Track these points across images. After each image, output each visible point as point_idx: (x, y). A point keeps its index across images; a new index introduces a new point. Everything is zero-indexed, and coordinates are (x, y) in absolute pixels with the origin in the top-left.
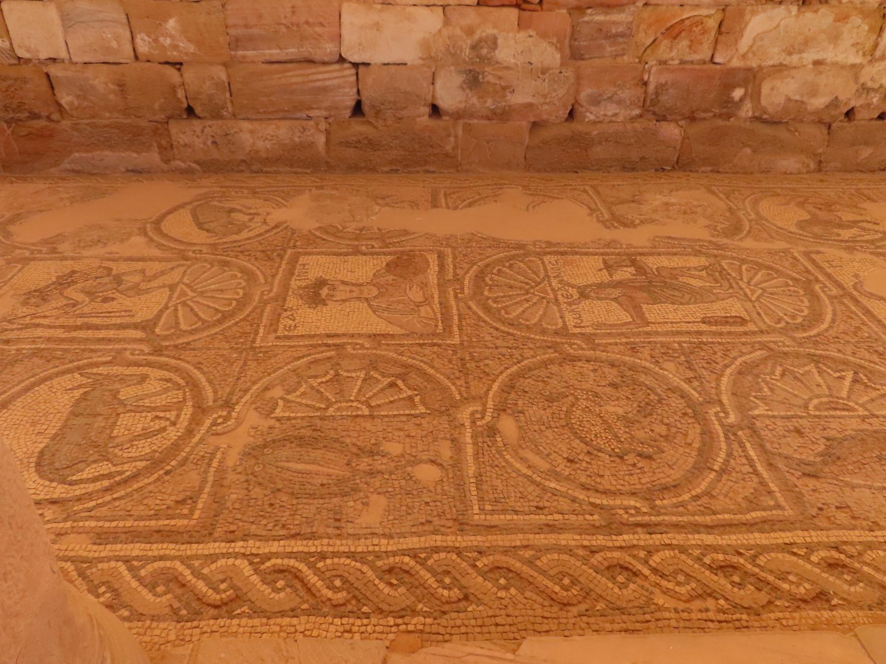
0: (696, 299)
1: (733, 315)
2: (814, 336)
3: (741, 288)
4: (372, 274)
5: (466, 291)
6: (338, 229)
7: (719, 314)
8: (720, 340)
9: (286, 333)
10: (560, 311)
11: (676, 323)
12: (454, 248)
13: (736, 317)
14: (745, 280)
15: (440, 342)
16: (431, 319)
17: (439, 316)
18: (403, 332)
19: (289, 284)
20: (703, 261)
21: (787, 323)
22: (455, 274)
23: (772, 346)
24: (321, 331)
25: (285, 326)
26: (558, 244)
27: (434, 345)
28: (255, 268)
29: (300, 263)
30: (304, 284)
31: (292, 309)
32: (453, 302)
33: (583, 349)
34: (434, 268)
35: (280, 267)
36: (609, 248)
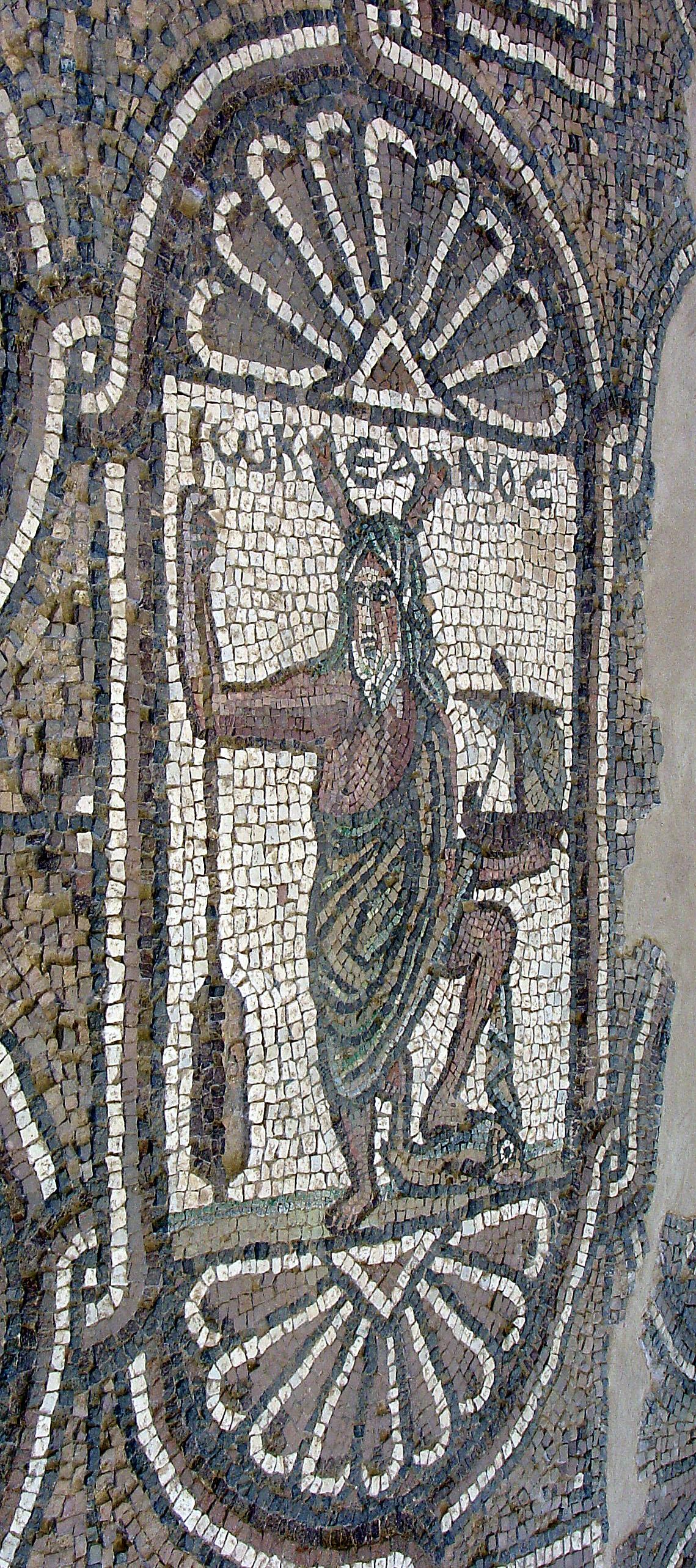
0: (339, 1007)
1: (257, 1138)
2: (132, 1446)
3: (396, 1231)
5: (394, 52)
7: (255, 1072)
8: (115, 1014)
10: (284, 394)
11: (210, 861)
13: (247, 1146)
14: (439, 1264)
20: (544, 1123)
21: (208, 1356)
23: (81, 1242)
26: (636, 557)
33: (74, 387)
36: (614, 760)
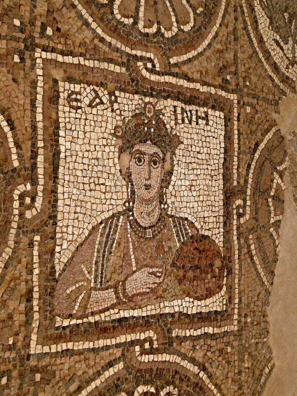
4: (182, 215)
5: (146, 358)
6: (280, 164)
12: (238, 334)
15: (35, 325)
16: (85, 308)
17: (91, 319)
19: (166, 98)
22: (182, 340)
24: (64, 144)
27: (29, 312)
28: (200, 49)
29: (210, 112)
30: (165, 119)
31: (112, 103)
32: (122, 339)
35: (204, 84)
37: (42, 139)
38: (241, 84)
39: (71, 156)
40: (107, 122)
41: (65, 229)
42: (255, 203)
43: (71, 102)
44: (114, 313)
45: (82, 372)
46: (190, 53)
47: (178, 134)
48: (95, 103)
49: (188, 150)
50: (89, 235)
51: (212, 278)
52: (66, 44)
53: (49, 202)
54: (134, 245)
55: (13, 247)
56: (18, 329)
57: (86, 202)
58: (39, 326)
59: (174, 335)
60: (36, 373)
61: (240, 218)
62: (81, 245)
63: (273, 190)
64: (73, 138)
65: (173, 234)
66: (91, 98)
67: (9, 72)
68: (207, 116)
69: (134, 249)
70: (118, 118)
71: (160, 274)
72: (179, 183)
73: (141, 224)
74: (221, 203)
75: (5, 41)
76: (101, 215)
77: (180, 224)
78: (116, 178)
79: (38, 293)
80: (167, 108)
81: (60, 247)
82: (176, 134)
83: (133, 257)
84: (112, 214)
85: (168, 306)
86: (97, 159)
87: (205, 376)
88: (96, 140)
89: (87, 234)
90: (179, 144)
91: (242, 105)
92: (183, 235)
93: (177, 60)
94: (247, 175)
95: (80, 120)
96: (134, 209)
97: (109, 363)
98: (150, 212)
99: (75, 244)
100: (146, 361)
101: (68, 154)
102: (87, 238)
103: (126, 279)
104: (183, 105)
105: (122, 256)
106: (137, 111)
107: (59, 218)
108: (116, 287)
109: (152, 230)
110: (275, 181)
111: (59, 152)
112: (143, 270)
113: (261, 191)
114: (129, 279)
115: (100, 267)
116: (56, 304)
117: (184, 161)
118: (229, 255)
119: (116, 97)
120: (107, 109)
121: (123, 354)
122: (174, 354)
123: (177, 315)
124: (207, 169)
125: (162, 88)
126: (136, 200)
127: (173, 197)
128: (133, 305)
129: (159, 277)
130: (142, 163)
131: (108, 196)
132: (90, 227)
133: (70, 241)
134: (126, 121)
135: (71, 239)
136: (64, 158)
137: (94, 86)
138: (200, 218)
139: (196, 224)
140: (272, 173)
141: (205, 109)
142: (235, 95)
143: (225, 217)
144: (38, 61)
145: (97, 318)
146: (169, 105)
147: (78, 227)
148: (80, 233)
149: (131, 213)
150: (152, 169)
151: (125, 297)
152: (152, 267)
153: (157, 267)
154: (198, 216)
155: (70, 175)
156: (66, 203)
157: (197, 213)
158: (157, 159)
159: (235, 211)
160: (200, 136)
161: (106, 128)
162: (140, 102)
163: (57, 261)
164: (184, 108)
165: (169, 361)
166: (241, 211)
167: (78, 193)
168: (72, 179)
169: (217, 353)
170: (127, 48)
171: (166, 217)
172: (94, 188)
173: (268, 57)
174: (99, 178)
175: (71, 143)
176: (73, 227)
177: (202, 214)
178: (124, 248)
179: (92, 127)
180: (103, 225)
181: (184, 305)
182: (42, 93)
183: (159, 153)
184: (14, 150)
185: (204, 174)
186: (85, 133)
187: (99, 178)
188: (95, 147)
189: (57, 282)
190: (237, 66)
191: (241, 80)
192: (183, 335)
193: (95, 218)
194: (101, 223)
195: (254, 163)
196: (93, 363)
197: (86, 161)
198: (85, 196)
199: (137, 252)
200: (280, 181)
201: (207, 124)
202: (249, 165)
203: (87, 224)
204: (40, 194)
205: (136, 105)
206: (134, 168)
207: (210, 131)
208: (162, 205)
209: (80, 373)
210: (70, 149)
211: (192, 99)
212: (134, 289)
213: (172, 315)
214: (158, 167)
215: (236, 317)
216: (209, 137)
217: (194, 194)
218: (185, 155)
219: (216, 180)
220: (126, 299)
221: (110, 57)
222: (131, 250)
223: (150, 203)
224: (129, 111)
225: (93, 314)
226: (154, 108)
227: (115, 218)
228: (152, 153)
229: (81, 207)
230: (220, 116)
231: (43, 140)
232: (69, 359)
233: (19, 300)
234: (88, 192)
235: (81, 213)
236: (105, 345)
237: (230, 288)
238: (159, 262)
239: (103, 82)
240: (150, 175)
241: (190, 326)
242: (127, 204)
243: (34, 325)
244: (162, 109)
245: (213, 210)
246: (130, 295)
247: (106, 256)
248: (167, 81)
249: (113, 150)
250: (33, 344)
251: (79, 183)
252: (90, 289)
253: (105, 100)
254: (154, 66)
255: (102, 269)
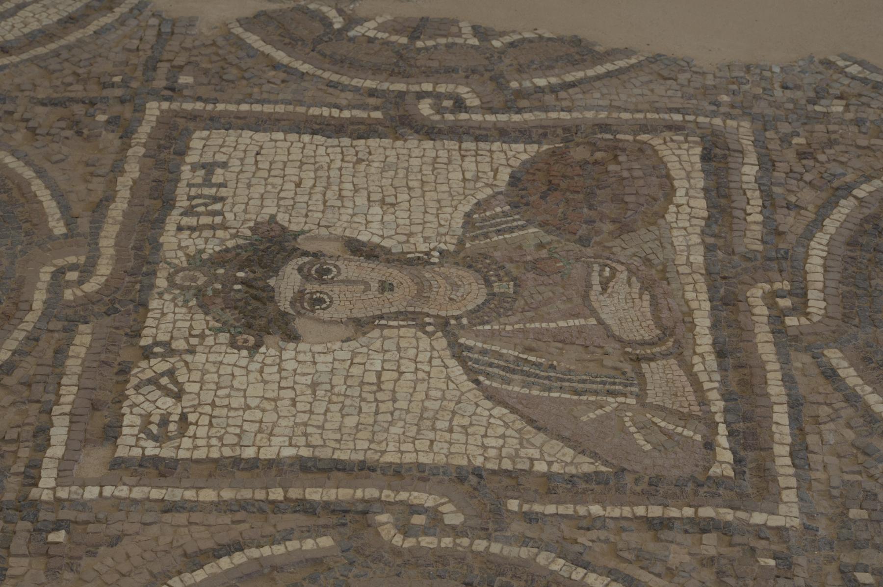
4: (458, 222)
5: (816, 304)
6: (326, 22)
9: (151, 449)
12: (764, 124)
15: (728, 515)
16: (691, 416)
17: (718, 406)
18: (587, 466)
19: (157, 247)
22: (774, 231)
24: (279, 448)
25: (146, 419)
28: (28, 173)
30: (212, 248)
31: (172, 352)
32: (767, 350)
34: (689, 204)
35: (117, 169)
37: (264, 492)
38: (118, 92)
39: (305, 435)
40: (221, 363)
41: (492, 453)
42: (428, 74)
43: (169, 434)
44: (703, 363)
45: (849, 431)
46: (38, 193)
47: (252, 224)
48: (171, 386)
49: (293, 206)
50: (506, 405)
51: (619, 163)
52: (17, 441)
53: (425, 480)
54: (532, 320)
55: (535, 550)
56: (738, 548)
57: (424, 409)
58: (732, 508)
59: (759, 247)
60: (847, 517)
61: (466, 107)
62: (531, 422)
63: (394, 38)
64: (260, 431)
65: (505, 239)
66: (158, 393)
67: (92, 554)
68: (203, 166)
69: (542, 319)
70: (210, 341)
71: (607, 269)
72: (375, 227)
73: (480, 301)
74: (428, 144)
75: (11, 559)
76: (458, 382)
77: (481, 228)
78: (365, 350)
79: (650, 507)
80: (183, 244)
81: (535, 462)
82: (250, 228)
83: (562, 324)
84: (454, 361)
85: (688, 258)
86: (314, 386)
87: (864, 186)
88: (267, 387)
89: (505, 411)
90: (276, 223)
91: (173, 91)
92: (506, 222)
93: (58, 220)
94: (356, 90)
95: (215, 417)
96: (443, 313)
97: (827, 377)
98: (451, 284)
99: (529, 432)
100: (823, 304)
101: (302, 441)
102: (513, 410)
103: (620, 340)
104: (175, 212)
105: (560, 345)
106: (190, 304)
107: (464, 462)
108: (639, 359)
109: (495, 282)
110: (371, 34)
111: (300, 458)
112: (596, 305)
113: (401, 64)
114: (617, 333)
115: (588, 386)
116: (676, 472)
117: (320, 215)
118: (559, 131)
119: (156, 344)
120: (187, 363)
121: (807, 349)
122: (807, 247)
123: (710, 240)
124: (340, 169)
125: (133, 252)
126: (418, 310)
127: (412, 240)
128: (680, 330)
129: (614, 271)
130: (325, 297)
131: (408, 366)
132: (488, 404)
133: (521, 444)
134: (217, 325)
135: (516, 441)
136: (311, 449)
137: (128, 386)
138: (464, 188)
139: (481, 196)
140: (352, 40)
141: (186, 168)
142: (148, 105)
143: (465, 137)
144: (63, 494)
145: (714, 395)
146: (174, 240)
147: (487, 428)
148: (502, 423)
149: (453, 322)
150: (340, 278)
151: (660, 341)
152: (589, 286)
153: (589, 275)
154: (461, 191)
155: (355, 439)
156: (427, 449)
157: (454, 194)
158: (314, 268)
159: (450, 117)
160: (254, 181)
161: (235, 365)
162: (167, 296)
163: (572, 470)
164: (182, 210)
165: (825, 258)
166: (448, 103)
167: (401, 424)
168: (364, 435)
169: (809, 163)
170: (27, 318)
171: (462, 255)
172: (390, 394)
173: (46, 35)
174: (362, 384)
175: (274, 435)
176: (485, 436)
177: (457, 185)
178: (540, 340)
179: (233, 393)
180: (481, 378)
181: (687, 224)
182: (146, 489)
183: (300, 263)
184: (293, 545)
185: (354, 176)
186: (248, 407)
187: (362, 384)
188: (284, 388)
189: (623, 470)
190: (72, 100)
191: (106, 93)
192: (758, 228)
193: (463, 394)
194: (477, 382)
195: (326, 75)
196: (826, 408)
197: (320, 408)
198: (408, 411)
199: (549, 314)
200: (372, 24)
201: (224, 165)
202: (331, 84)
203: (479, 410)
204: (403, 496)
205: (176, 305)
206: (339, 310)
207: (242, 160)
208: (432, 260)
209: (850, 435)
210: (291, 438)
211: (158, 196)
212: (644, 324)
213: (709, 249)
214: (336, 266)
215: (718, 121)
216: (256, 162)
217: (403, 197)
218: (304, 212)
219: (370, 153)
220: (668, 341)
221: (50, 353)
222: (544, 325)
223: (426, 283)
224: (192, 319)
225: (703, 402)
226: (183, 269)
227: (464, 354)
228: (299, 277)
229: (437, 419)
230: (203, 139)
231: (267, 488)
232: (812, 452)
233: (667, 544)
234: (397, 405)
235: (451, 420)
236: (781, 383)
237: (644, 128)
238: (577, 270)
239: (115, 370)
240: (355, 282)
241: (737, 213)
242: (430, 329)
243: (730, 517)
244: (187, 255)
245: (446, 161)
246: (658, 332)
247: (560, 376)
248: (112, 242)
249: (294, 353)
250: (775, 521)
251: (375, 422)
252: (643, 405)
253: (164, 366)
254: (73, 267)
255: (593, 383)
